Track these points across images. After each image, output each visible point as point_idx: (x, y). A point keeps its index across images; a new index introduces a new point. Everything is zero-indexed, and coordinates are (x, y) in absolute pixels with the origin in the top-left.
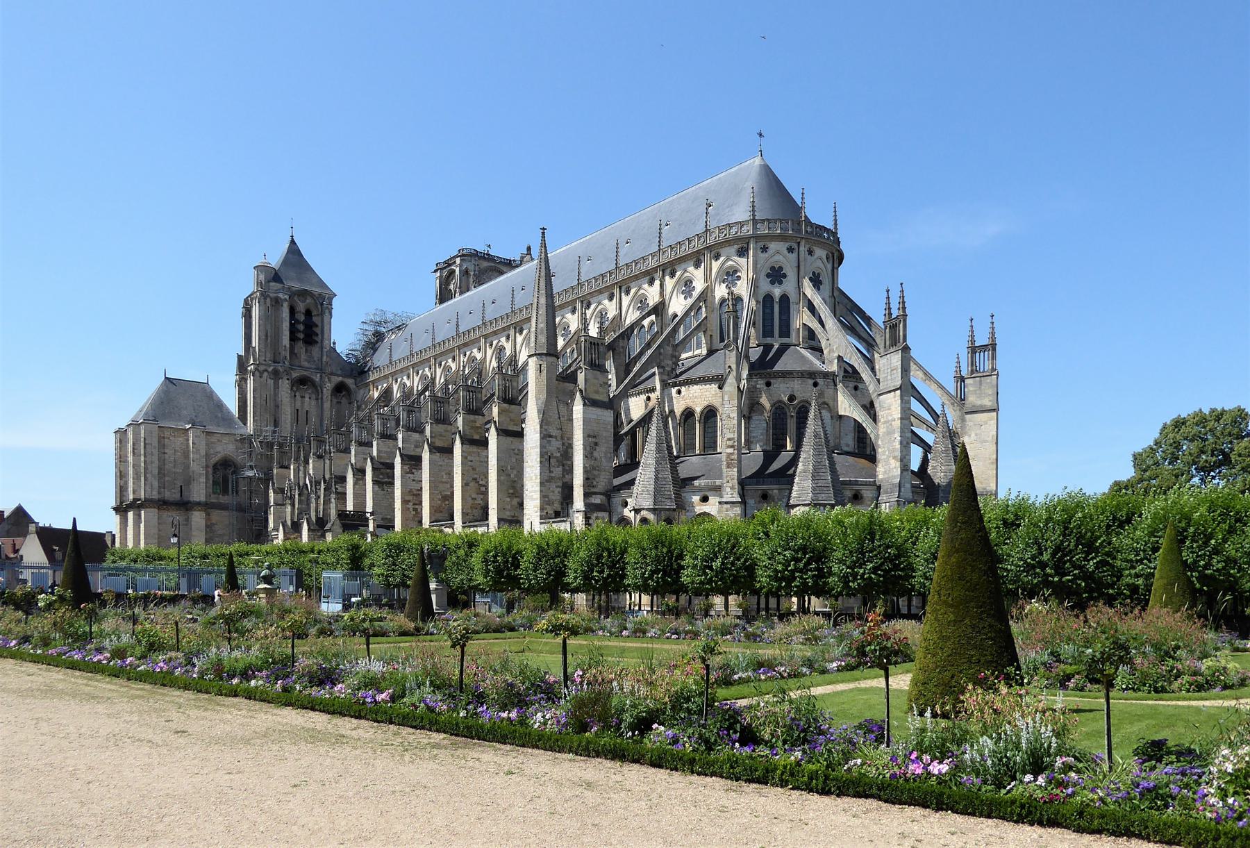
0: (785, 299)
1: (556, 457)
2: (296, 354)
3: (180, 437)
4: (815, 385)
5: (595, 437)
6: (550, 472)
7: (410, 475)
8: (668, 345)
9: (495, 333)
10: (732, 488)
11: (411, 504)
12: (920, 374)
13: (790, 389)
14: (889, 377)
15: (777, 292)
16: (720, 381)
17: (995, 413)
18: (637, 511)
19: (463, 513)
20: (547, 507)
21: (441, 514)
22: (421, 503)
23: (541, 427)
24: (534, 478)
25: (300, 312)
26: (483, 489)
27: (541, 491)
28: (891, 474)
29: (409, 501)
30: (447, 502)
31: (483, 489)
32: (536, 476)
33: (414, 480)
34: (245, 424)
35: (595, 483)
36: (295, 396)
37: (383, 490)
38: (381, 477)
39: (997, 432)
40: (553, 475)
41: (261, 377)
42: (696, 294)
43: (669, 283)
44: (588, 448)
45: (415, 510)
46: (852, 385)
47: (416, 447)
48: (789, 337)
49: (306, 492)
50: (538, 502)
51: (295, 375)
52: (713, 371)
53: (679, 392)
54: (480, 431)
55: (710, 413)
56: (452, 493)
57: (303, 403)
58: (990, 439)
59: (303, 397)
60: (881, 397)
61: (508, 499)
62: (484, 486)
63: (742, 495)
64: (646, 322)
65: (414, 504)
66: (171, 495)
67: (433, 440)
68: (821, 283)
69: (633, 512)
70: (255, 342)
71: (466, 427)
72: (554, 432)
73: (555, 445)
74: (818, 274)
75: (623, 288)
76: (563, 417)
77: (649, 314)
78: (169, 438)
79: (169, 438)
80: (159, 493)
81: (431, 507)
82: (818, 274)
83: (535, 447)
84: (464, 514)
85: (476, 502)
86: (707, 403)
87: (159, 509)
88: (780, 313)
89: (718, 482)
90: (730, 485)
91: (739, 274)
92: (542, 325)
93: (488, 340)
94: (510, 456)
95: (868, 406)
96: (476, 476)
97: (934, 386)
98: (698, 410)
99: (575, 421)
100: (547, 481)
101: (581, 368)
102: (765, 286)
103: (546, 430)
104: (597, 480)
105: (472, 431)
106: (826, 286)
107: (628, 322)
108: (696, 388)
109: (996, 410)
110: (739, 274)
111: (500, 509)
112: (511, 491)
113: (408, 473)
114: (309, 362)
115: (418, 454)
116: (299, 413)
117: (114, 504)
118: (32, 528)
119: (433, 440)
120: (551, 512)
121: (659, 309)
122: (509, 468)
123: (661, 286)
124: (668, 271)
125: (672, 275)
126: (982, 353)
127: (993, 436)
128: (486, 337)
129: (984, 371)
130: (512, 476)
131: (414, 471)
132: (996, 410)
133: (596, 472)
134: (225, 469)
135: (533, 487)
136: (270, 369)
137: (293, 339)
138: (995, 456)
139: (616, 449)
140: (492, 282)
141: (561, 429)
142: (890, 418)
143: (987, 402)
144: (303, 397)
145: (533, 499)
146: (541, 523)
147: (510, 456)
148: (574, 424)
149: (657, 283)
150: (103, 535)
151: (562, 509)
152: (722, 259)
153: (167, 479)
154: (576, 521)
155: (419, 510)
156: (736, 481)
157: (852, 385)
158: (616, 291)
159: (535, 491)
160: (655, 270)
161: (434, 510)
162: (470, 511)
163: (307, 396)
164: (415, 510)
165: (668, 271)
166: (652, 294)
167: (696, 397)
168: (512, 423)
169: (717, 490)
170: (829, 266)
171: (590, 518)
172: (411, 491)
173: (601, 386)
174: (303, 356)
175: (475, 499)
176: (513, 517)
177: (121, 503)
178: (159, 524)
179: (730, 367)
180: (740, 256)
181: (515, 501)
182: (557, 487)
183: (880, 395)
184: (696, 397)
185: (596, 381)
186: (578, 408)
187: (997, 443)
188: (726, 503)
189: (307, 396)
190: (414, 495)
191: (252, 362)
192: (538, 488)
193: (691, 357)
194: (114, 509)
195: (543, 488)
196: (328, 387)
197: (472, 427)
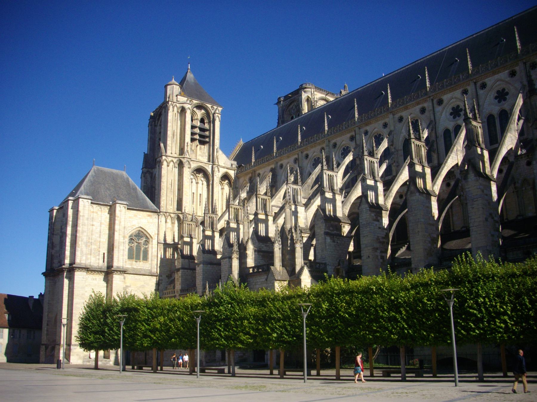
7: (377, 223)
11: (379, 251)
29: (377, 249)
36: (192, 182)
37: (334, 241)
38: (331, 228)
41: (168, 166)
51: (194, 165)
57: (197, 188)
59: (197, 183)
78: (97, 213)
79: (97, 213)
80: (87, 259)
113: (375, 220)
114: (202, 156)
116: (195, 195)
117: (44, 271)
134: (139, 239)
136: (175, 160)
137: (193, 140)
144: (197, 183)
153: (93, 247)
163: (200, 182)
172: (378, 239)
189: (200, 182)
190: (380, 242)
196: (218, 176)
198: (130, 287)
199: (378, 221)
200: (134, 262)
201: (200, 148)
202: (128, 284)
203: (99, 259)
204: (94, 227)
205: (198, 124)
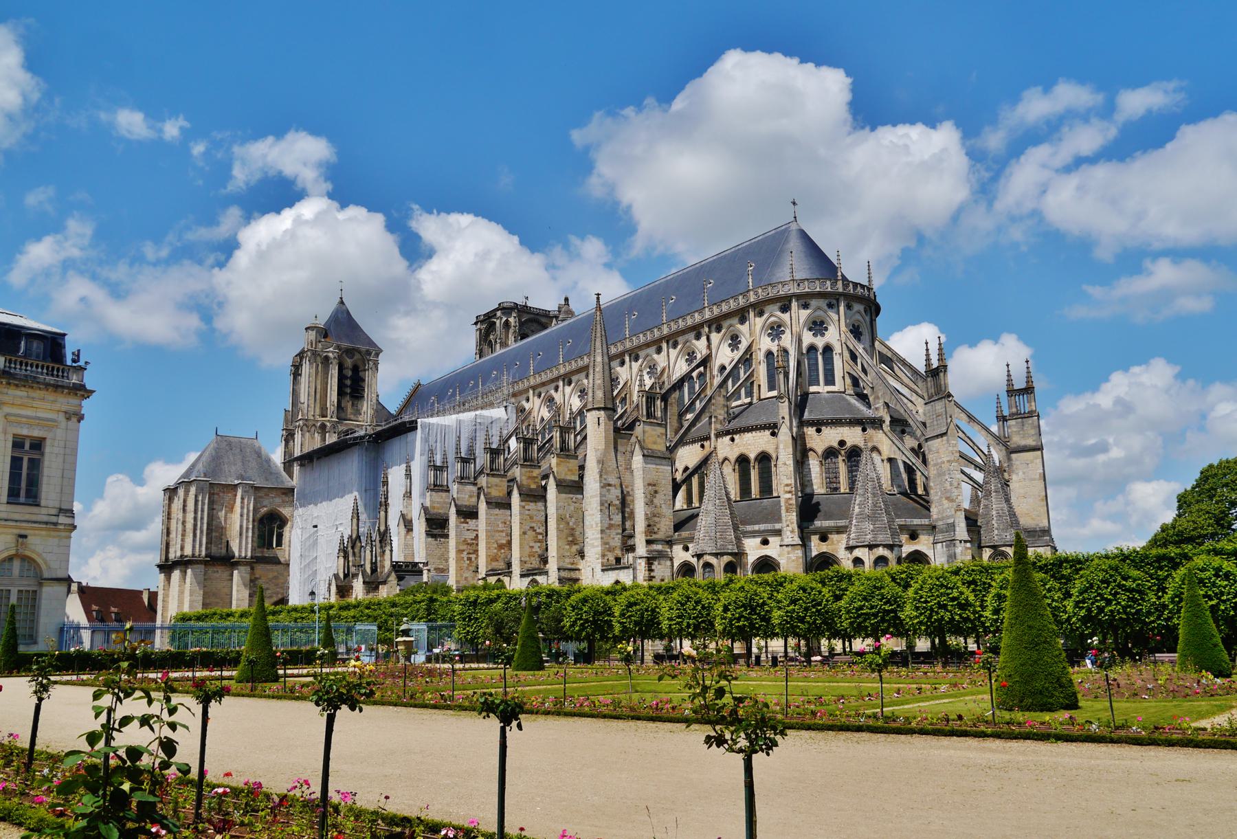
0: (828, 349)
1: (614, 505)
2: (343, 409)
3: (229, 492)
4: (864, 430)
5: (654, 485)
6: (610, 519)
8: (719, 396)
9: (543, 384)
10: (792, 532)
11: (465, 553)
12: (963, 416)
13: (840, 435)
14: (935, 423)
15: (820, 342)
16: (773, 429)
17: (1040, 452)
18: (699, 556)
19: (521, 561)
20: (608, 553)
21: (496, 563)
22: (476, 552)
23: (601, 476)
24: (594, 526)
25: (347, 368)
26: (540, 537)
27: (602, 538)
28: (944, 515)
29: (464, 551)
30: (503, 551)
31: (540, 537)
32: (597, 524)
33: (468, 530)
34: (292, 478)
35: (656, 529)
37: (436, 540)
39: (1044, 470)
40: (612, 522)
42: (743, 346)
43: (715, 337)
44: (649, 496)
45: (469, 559)
46: (899, 429)
47: (471, 496)
48: (834, 384)
49: (359, 544)
50: (599, 549)
52: (764, 420)
53: (733, 440)
54: (536, 480)
55: (764, 459)
56: (510, 543)
58: (1038, 476)
60: (929, 443)
61: (568, 547)
62: (541, 534)
63: (802, 538)
64: (694, 374)
65: (469, 553)
66: (219, 551)
67: (489, 490)
68: (861, 334)
69: (695, 559)
70: (303, 397)
71: (524, 478)
72: (613, 480)
73: (615, 493)
74: (858, 326)
75: (671, 343)
76: (621, 466)
77: (698, 366)
78: (218, 494)
79: (218, 494)
81: (488, 556)
82: (858, 326)
83: (595, 496)
84: (523, 562)
85: (534, 550)
86: (760, 450)
87: (205, 565)
88: (825, 364)
89: (777, 526)
90: (790, 528)
91: (782, 329)
92: (599, 382)
93: (537, 391)
94: (569, 505)
95: (916, 448)
96: (533, 525)
97: (977, 427)
98: (752, 456)
99: (635, 471)
100: (607, 528)
101: (639, 421)
102: (808, 338)
103: (605, 479)
104: (658, 526)
105: (529, 481)
106: (866, 337)
107: (677, 375)
108: (748, 436)
109: (1039, 448)
110: (782, 329)
111: (561, 557)
112: (570, 539)
113: (463, 523)
115: (472, 504)
117: (158, 561)
118: (74, 587)
119: (489, 490)
120: (612, 560)
121: (705, 362)
122: (568, 516)
123: (708, 339)
124: (714, 327)
125: (719, 330)
126: (1021, 397)
127: (1040, 474)
128: (534, 388)
129: (1025, 413)
130: (571, 524)
131: (468, 520)
132: (1039, 448)
133: (656, 519)
135: (593, 534)
137: (341, 393)
138: (1044, 494)
139: (674, 496)
140: (537, 336)
141: (620, 478)
142: (939, 461)
143: (1031, 442)
145: (594, 546)
146: (603, 570)
147: (569, 505)
148: (635, 474)
149: (704, 339)
150: (141, 592)
151: (623, 555)
152: (765, 316)
153: (214, 534)
154: (638, 567)
155: (473, 559)
156: (795, 526)
157: (899, 429)
158: (664, 345)
159: (596, 539)
160: (701, 325)
161: (492, 559)
162: (528, 559)
164: (469, 559)
165: (714, 327)
166: (700, 346)
167: (749, 445)
168: (569, 473)
169: (778, 533)
170: (868, 319)
171: (652, 564)
172: (465, 541)
173: (659, 436)
174: (349, 410)
175: (532, 547)
176: (572, 564)
177: (167, 559)
178: (205, 580)
179: (783, 418)
180: (783, 312)
181: (575, 548)
182: (617, 534)
183: (927, 440)
184: (749, 445)
185: (654, 433)
186: (638, 460)
187: (1045, 480)
188: (787, 546)
190: (468, 544)
191: (300, 417)
192: (599, 536)
193: (741, 405)
194: (159, 566)
195: (603, 535)
197: (530, 478)
198: (259, 578)
199: (467, 523)
200: (265, 550)
201: (353, 405)
202: (257, 576)
203: (221, 548)
204: (215, 511)
205: (349, 373)
